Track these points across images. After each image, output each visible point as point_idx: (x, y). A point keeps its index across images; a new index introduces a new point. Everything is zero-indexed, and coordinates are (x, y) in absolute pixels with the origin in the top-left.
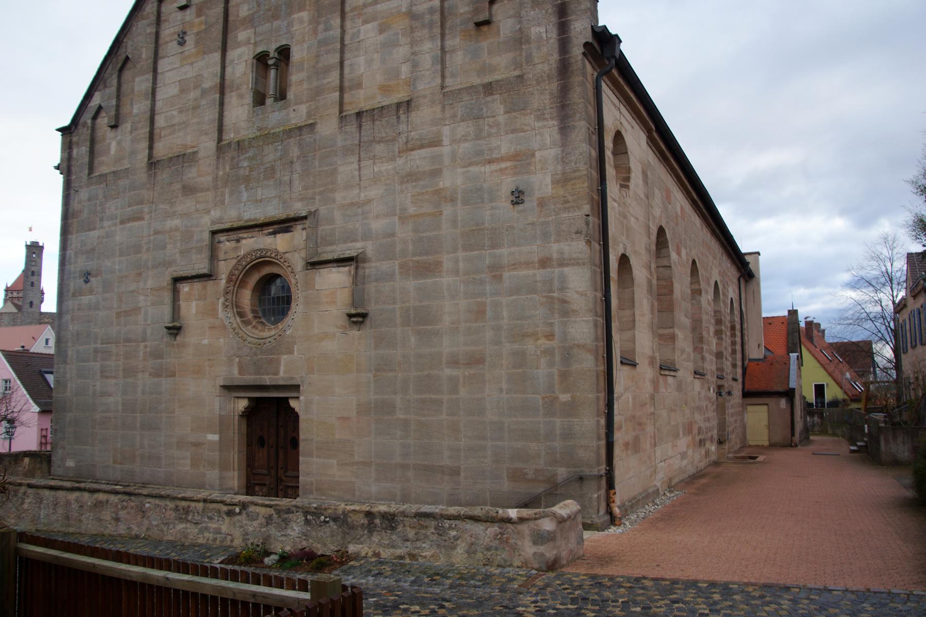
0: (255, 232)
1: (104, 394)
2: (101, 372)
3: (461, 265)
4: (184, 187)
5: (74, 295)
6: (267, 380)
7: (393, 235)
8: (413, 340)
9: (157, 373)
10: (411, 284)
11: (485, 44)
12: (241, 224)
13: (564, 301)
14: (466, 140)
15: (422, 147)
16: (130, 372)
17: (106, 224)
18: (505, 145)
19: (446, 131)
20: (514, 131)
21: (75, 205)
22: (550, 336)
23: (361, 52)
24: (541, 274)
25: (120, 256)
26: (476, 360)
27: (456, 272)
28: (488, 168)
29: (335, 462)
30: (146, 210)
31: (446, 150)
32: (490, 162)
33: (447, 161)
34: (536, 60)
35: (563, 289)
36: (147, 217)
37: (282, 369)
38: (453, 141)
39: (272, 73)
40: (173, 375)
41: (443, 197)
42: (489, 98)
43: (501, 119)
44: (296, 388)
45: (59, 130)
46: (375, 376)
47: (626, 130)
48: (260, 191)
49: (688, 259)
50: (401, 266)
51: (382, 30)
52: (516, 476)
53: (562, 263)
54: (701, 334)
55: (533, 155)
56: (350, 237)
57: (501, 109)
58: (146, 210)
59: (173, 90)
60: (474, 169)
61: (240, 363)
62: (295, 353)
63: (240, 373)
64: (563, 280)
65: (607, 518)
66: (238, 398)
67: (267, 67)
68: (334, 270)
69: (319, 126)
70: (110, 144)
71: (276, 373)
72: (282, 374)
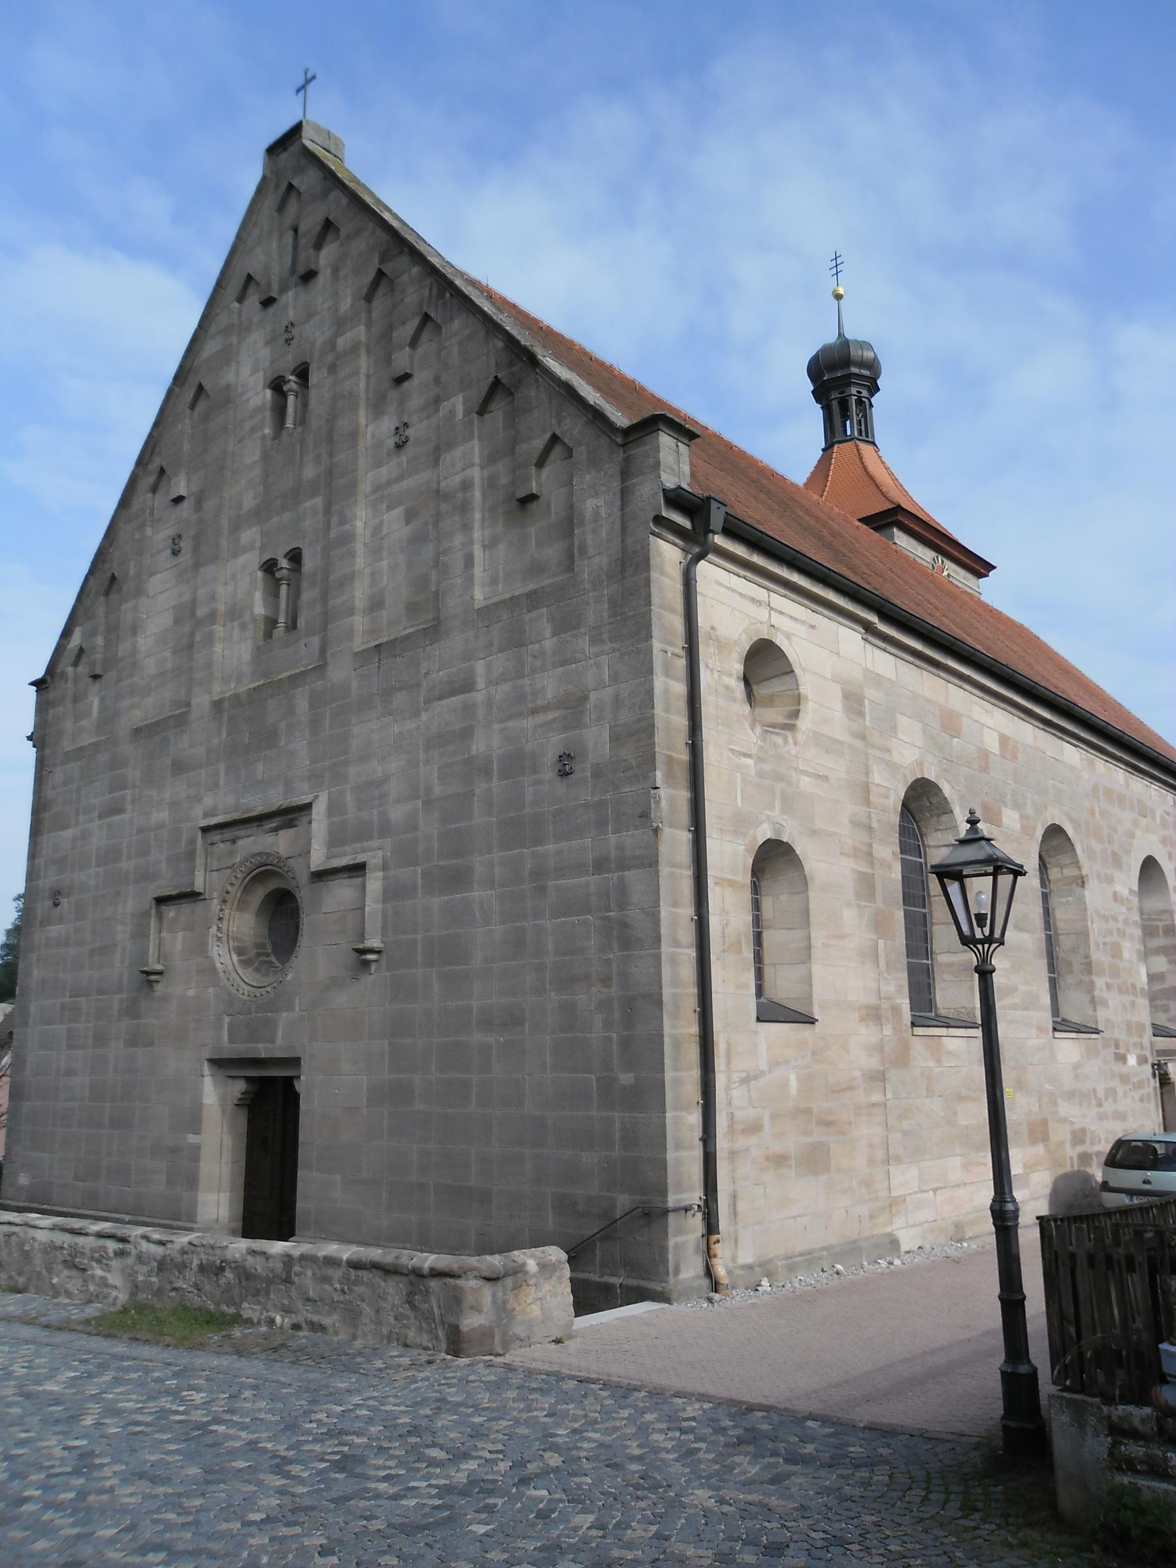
0: (253, 829)
1: (70, 1072)
2: (69, 1039)
3: (497, 871)
4: (174, 763)
5: (41, 925)
6: (262, 1050)
7: (415, 828)
8: (436, 988)
9: (136, 1040)
10: (436, 902)
11: (532, 530)
12: (237, 816)
13: (624, 925)
14: (505, 680)
15: (452, 693)
16: (101, 1039)
17: (81, 819)
18: (549, 685)
19: (480, 667)
20: (564, 663)
21: (49, 793)
22: (606, 981)
23: (385, 554)
24: (593, 881)
25: (97, 865)
26: (513, 1019)
27: (490, 883)
28: (529, 723)
29: (337, 1178)
30: (129, 798)
31: (479, 696)
32: (534, 712)
33: (481, 712)
34: (591, 551)
35: (622, 906)
36: (129, 807)
37: (280, 1033)
38: (489, 683)
39: (284, 589)
40: (151, 1044)
41: (479, 768)
42: (534, 614)
43: (549, 644)
44: (295, 1062)
45: (33, 684)
46: (390, 1044)
47: (788, 636)
48: (260, 767)
49: (1027, 830)
50: (425, 874)
51: (410, 516)
52: (565, 1206)
53: (622, 866)
54: (1087, 957)
55: (586, 698)
56: (363, 834)
57: (548, 631)
58: (129, 798)
59: (167, 620)
60: (513, 724)
61: (231, 1025)
62: (297, 1008)
63: (232, 1039)
64: (623, 888)
65: (705, 1282)
66: (233, 1077)
67: (277, 582)
68: (346, 882)
69: (330, 668)
70: (91, 703)
71: (272, 1041)
72: (279, 1041)
